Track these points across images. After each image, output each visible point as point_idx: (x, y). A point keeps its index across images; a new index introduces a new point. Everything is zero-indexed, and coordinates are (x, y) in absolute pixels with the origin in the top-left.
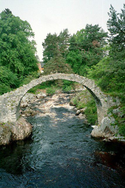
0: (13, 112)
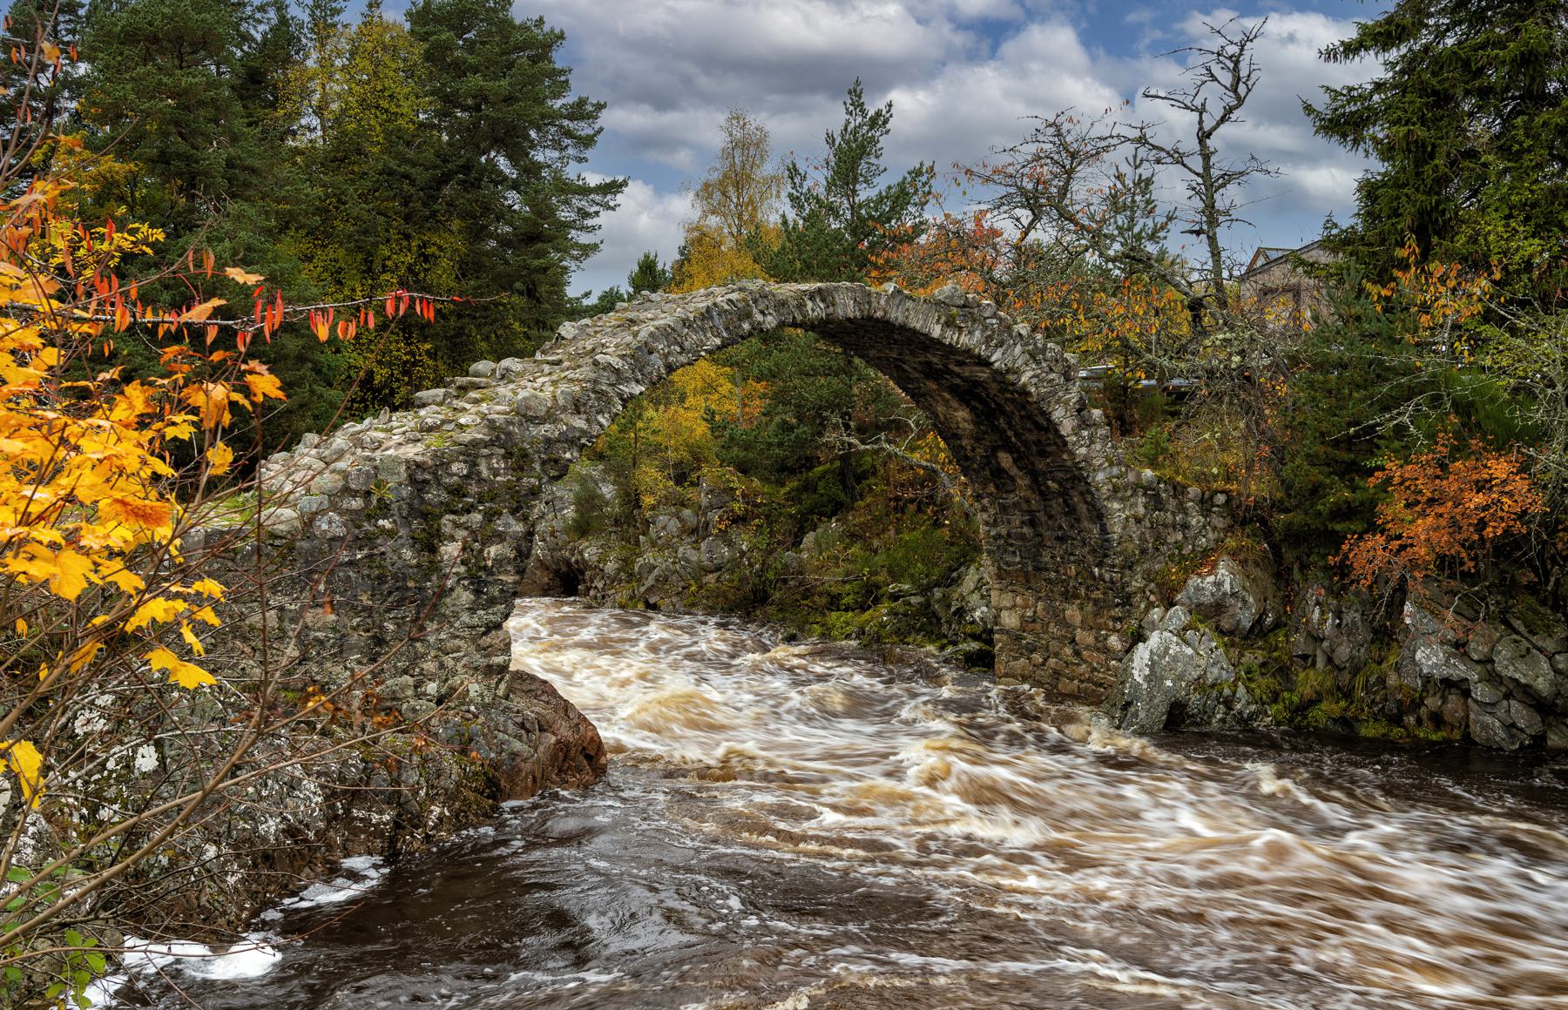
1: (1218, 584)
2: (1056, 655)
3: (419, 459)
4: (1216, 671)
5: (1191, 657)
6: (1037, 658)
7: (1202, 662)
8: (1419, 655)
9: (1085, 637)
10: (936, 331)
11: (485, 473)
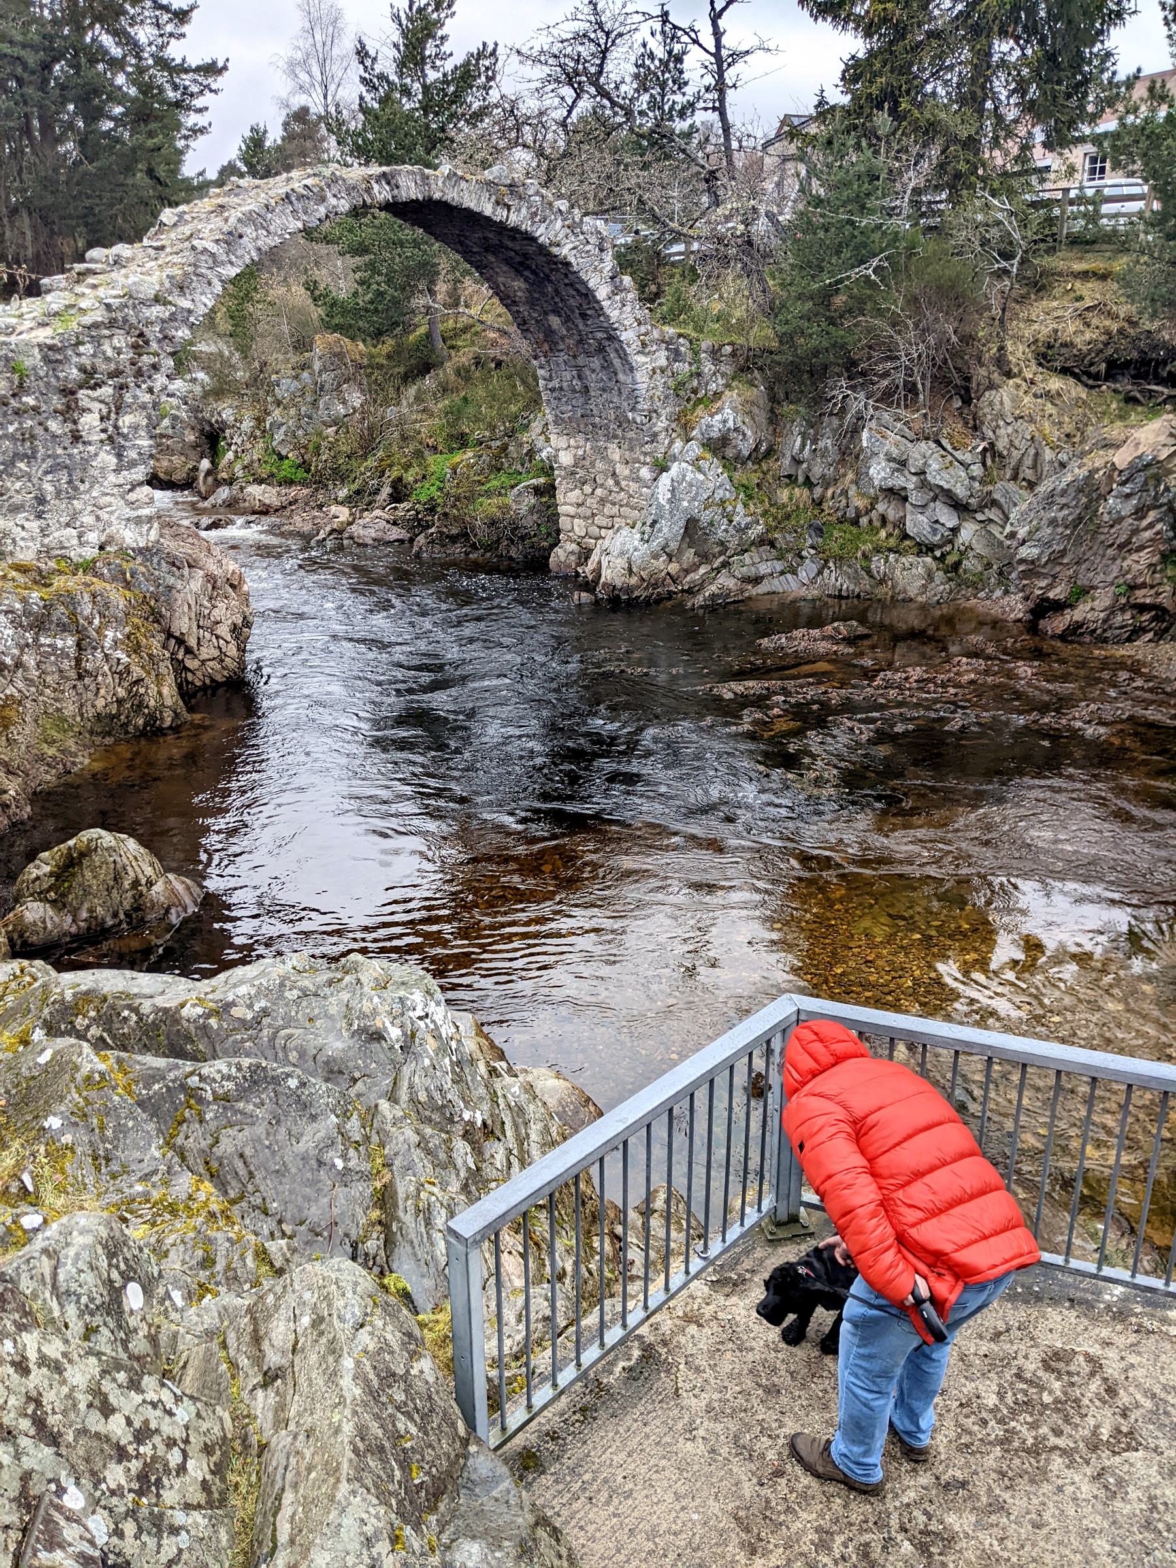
0: (133, 464)
1: (725, 421)
2: (602, 485)
3: (49, 342)
4: (721, 492)
5: (702, 482)
6: (588, 489)
7: (711, 485)
8: (871, 471)
9: (622, 470)
10: (488, 209)
11: (110, 353)
